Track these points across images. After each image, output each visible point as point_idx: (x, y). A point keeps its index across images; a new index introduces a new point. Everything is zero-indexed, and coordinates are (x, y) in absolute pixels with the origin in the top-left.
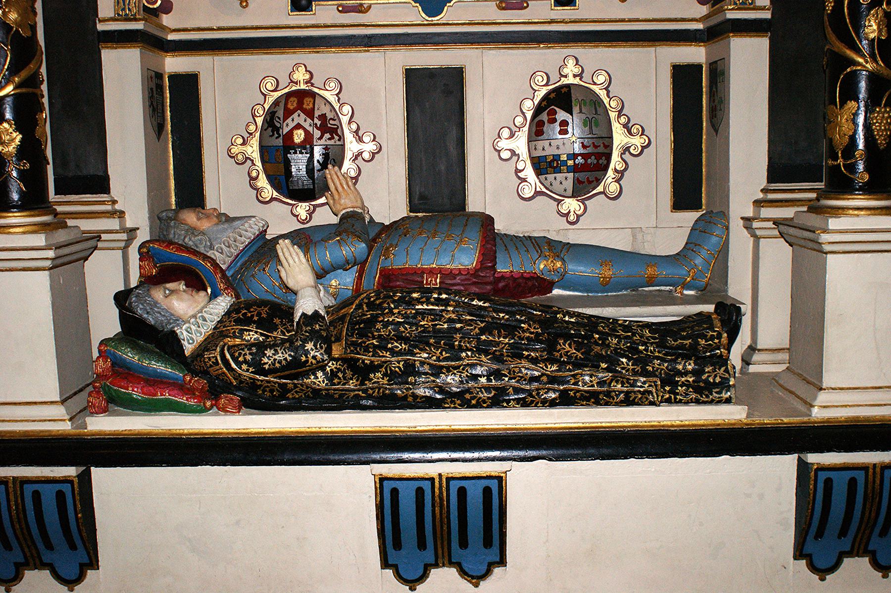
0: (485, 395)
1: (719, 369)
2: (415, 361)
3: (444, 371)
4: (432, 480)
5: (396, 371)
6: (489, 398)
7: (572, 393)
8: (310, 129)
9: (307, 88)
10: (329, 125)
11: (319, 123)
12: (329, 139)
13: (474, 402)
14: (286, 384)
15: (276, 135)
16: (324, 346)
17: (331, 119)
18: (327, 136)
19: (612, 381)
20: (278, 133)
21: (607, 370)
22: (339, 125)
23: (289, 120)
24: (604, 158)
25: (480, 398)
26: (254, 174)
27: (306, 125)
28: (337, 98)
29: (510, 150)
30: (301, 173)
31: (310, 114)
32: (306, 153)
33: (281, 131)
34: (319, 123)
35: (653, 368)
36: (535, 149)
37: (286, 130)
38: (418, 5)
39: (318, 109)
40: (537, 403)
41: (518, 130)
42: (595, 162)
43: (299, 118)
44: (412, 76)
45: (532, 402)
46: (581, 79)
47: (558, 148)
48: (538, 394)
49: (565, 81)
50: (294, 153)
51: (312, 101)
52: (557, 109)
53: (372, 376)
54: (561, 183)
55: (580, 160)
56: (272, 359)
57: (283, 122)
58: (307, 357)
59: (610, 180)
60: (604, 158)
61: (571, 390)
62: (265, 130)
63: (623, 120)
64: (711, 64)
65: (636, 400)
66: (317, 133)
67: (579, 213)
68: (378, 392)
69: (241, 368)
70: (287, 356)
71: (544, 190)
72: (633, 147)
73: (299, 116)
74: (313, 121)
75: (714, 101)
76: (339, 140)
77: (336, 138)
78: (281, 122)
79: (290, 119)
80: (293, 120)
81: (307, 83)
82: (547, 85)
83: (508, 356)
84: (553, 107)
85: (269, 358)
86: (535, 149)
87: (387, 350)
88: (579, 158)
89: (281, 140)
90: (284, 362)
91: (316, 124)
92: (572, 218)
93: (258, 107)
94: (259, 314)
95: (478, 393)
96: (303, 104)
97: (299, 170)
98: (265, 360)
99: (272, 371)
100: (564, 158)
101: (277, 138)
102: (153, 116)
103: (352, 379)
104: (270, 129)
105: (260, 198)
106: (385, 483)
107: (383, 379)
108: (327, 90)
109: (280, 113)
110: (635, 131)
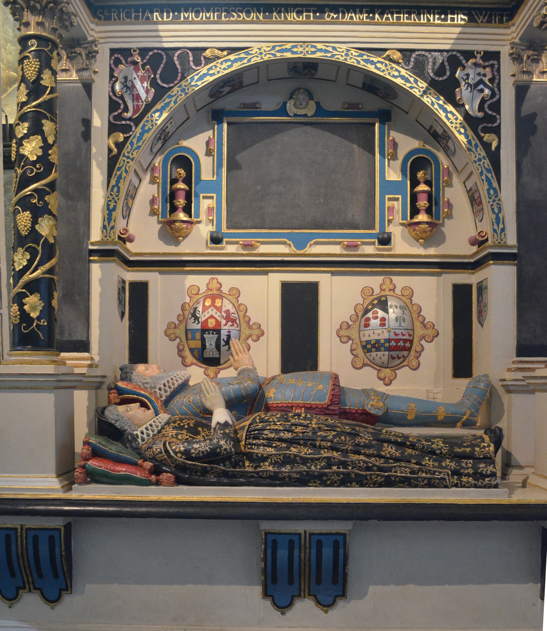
0: (335, 478)
1: (489, 466)
2: (291, 454)
3: (309, 461)
4: (300, 534)
5: (278, 461)
6: (339, 480)
7: (393, 478)
8: (219, 319)
11: (225, 315)
12: (231, 326)
13: (329, 482)
14: (206, 467)
15: (197, 322)
16: (232, 443)
17: (232, 313)
18: (230, 323)
19: (419, 471)
20: (198, 321)
21: (416, 464)
23: (206, 313)
24: (408, 343)
25: (333, 480)
26: (181, 348)
27: (217, 316)
29: (347, 336)
31: (219, 309)
33: (200, 320)
34: (225, 315)
35: (446, 464)
36: (364, 336)
37: (203, 319)
38: (291, 242)
40: (370, 484)
41: (352, 323)
42: (403, 344)
43: (212, 312)
44: (286, 287)
45: (367, 483)
46: (394, 292)
47: (379, 335)
48: (371, 478)
49: (383, 293)
50: (209, 334)
51: (221, 301)
52: (378, 310)
53: (262, 464)
54: (380, 358)
55: (393, 343)
56: (198, 451)
58: (220, 449)
59: (412, 358)
60: (408, 343)
61: (393, 476)
63: (421, 319)
64: (478, 283)
65: (435, 484)
66: (223, 322)
67: (391, 378)
68: (266, 475)
69: (177, 456)
70: (207, 448)
71: (369, 362)
72: (427, 337)
75: (480, 306)
76: (237, 327)
77: (236, 325)
79: (206, 312)
80: (208, 312)
81: (218, 290)
82: (372, 295)
83: (351, 453)
84: (376, 309)
85: (196, 449)
86: (364, 336)
87: (272, 447)
88: (393, 342)
89: (199, 325)
90: (205, 453)
91: (223, 316)
92: (387, 380)
94: (188, 424)
95: (331, 476)
96: (215, 303)
97: (211, 345)
98: (193, 451)
99: (197, 459)
100: (382, 341)
103: (248, 466)
104: (193, 318)
106: (269, 536)
107: (269, 466)
110: (429, 326)
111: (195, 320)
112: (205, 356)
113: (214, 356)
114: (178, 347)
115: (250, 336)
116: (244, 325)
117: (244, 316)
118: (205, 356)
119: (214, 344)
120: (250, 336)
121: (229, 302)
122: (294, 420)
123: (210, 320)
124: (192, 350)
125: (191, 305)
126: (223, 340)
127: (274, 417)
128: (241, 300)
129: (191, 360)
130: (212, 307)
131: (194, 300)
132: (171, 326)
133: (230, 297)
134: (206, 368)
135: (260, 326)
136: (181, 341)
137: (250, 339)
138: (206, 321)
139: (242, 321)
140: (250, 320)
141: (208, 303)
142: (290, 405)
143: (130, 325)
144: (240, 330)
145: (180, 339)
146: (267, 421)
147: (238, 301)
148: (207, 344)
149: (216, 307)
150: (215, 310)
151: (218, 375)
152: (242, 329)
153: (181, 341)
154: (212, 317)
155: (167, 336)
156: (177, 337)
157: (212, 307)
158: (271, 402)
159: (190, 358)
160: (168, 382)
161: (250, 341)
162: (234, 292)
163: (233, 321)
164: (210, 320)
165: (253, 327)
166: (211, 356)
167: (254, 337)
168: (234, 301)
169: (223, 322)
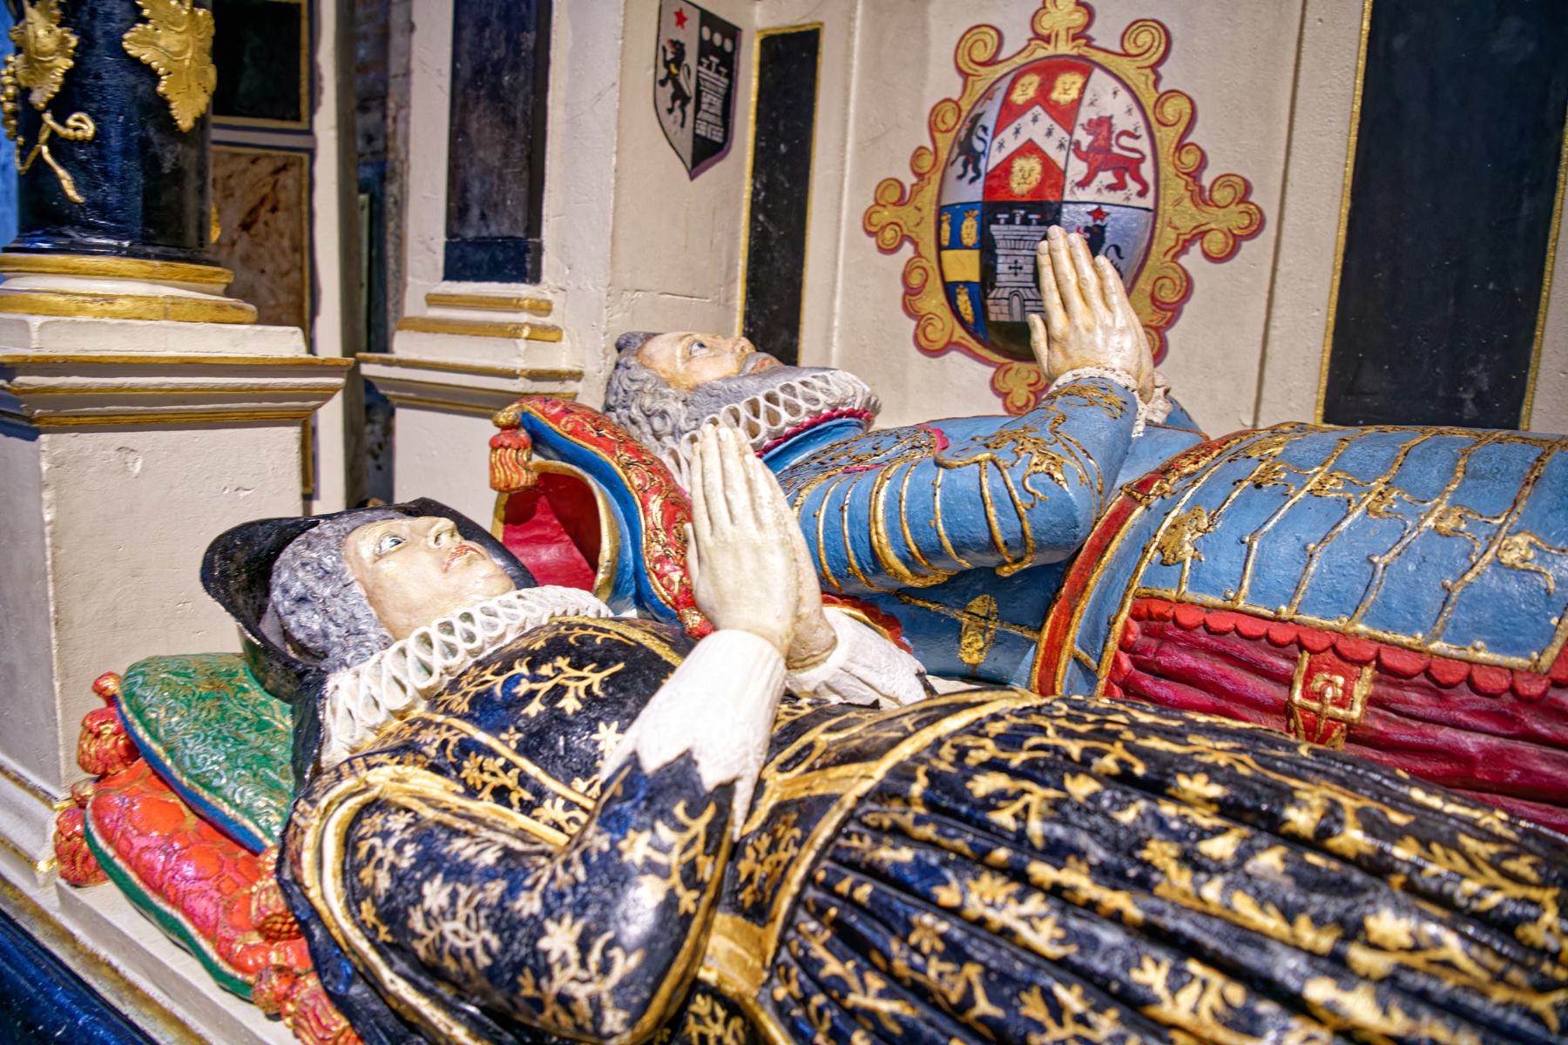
8: (1058, 157)
9: (1074, 52)
10: (1116, 150)
11: (1085, 140)
12: (1111, 187)
15: (971, 174)
20: (976, 170)
22: (1147, 150)
23: (1007, 134)
26: (916, 280)
28: (1152, 77)
30: (1019, 278)
31: (1065, 116)
33: (983, 161)
34: (1085, 140)
37: (995, 158)
39: (1092, 104)
43: (1036, 127)
50: (1010, 221)
57: (995, 135)
66: (1077, 169)
73: (1035, 120)
74: (1071, 133)
76: (1142, 194)
77: (1134, 187)
79: (1011, 130)
80: (1017, 131)
89: (980, 183)
91: (1078, 144)
93: (950, 106)
96: (1051, 89)
105: (924, 343)
108: (1127, 55)
111: (965, 166)
112: (993, 318)
114: (905, 278)
115: (1200, 235)
116: (1175, 187)
117: (1180, 147)
118: (993, 318)
120: (1200, 235)
121: (1115, 84)
122: (1182, 879)
123: (1019, 164)
125: (966, 106)
127: (1037, 796)
128: (1172, 75)
129: (948, 331)
130: (1038, 109)
131: (980, 87)
132: (893, 195)
133: (1126, 67)
135: (1248, 188)
137: (1195, 250)
138: (1005, 167)
139: (1168, 170)
140: (1203, 163)
142: (1280, 634)
143: (755, 193)
144: (1154, 212)
145: (915, 244)
146: (976, 815)
148: (1002, 267)
149: (1055, 110)
150: (1046, 121)
152: (1166, 207)
153: (918, 254)
154: (1030, 149)
155: (870, 234)
156: (905, 238)
157: (1038, 109)
158: (1173, 594)
159: (944, 326)
161: (1193, 260)
162: (1145, 38)
163: (1126, 168)
164: (1019, 164)
165: (1217, 196)
167: (1216, 242)
168: (1141, 82)
169: (1077, 169)
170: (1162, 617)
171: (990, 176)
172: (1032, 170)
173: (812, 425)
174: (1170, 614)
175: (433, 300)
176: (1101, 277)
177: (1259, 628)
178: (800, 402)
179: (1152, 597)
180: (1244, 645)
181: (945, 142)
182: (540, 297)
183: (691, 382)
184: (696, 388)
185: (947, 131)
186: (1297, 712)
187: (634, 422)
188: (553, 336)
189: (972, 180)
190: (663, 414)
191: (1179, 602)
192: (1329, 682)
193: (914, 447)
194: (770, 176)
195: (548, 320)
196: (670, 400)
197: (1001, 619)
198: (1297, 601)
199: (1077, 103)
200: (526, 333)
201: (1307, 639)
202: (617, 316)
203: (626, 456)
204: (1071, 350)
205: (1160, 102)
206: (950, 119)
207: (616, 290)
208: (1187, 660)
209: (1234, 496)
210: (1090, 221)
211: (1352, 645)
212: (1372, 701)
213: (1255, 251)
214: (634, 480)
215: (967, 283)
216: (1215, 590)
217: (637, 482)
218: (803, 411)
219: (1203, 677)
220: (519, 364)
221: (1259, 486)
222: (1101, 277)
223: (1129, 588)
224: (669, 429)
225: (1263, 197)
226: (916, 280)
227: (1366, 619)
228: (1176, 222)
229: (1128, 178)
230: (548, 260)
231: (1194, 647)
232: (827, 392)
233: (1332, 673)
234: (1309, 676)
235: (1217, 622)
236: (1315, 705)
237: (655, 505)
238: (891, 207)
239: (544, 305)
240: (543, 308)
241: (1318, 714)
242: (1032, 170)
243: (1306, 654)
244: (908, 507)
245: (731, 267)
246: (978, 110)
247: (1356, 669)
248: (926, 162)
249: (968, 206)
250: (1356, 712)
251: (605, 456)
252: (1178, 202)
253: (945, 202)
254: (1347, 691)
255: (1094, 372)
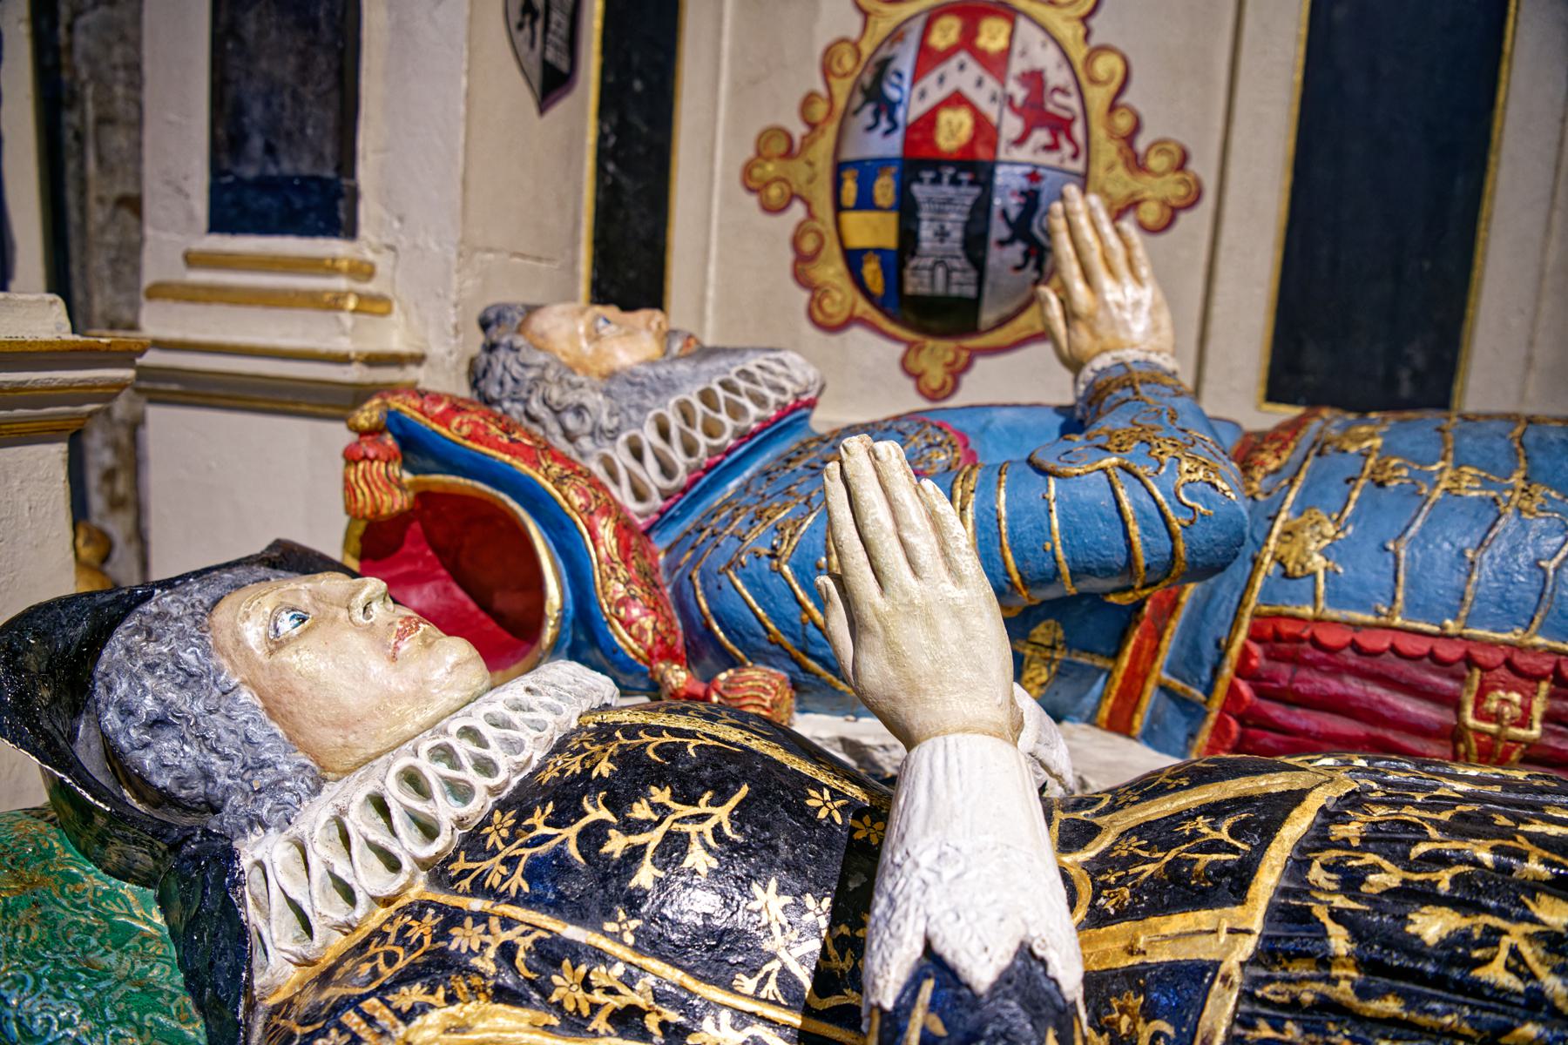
8: (991, 111)
10: (1050, 107)
11: (1020, 94)
15: (884, 125)
17: (1056, 89)
18: (1041, 136)
23: (930, 81)
26: (809, 245)
27: (981, 99)
28: (1081, 31)
31: (995, 64)
32: (972, 183)
33: (900, 114)
34: (1020, 94)
37: (917, 109)
43: (962, 75)
50: (937, 181)
62: (856, 112)
66: (1011, 126)
73: (962, 67)
74: (1003, 84)
76: (1075, 156)
77: (1067, 148)
78: (906, 86)
80: (941, 80)
89: (897, 139)
93: (846, 48)
101: (887, 133)
102: (520, 26)
104: (869, 108)
105: (819, 316)
109: (905, 61)
111: (876, 114)
113: (955, 291)
114: (796, 243)
117: (1113, 107)
119: (957, 234)
123: (945, 116)
124: (853, 259)
125: (867, 48)
126: (1004, 214)
129: (848, 306)
131: (883, 27)
134: (910, 345)
136: (811, 215)
138: (929, 121)
139: (1099, 133)
140: (1137, 127)
141: (946, 33)
142: (1447, 651)
143: (602, 138)
145: (808, 204)
147: (1087, 35)
148: (926, 231)
149: (981, 57)
150: (974, 70)
151: (967, 380)
153: (811, 215)
154: (957, 100)
155: (751, 190)
156: (793, 196)
157: (963, 56)
158: (1308, 611)
159: (842, 296)
160: (686, 412)
163: (1060, 126)
164: (945, 116)
166: (940, 289)
168: (1069, 31)
170: (1298, 639)
171: (910, 129)
172: (961, 125)
173: (779, 419)
174: (1307, 633)
175: (193, 260)
176: (1127, 246)
177: (1422, 646)
178: (766, 392)
179: (1279, 616)
180: (1404, 665)
181: (842, 88)
182: (358, 256)
183: (604, 367)
184: (611, 375)
185: (845, 75)
186: (1471, 736)
187: (533, 419)
188: (379, 308)
189: (887, 133)
190: (579, 410)
191: (1318, 620)
192: (1505, 701)
193: (930, 446)
194: (622, 118)
195: (371, 287)
196: (586, 390)
197: (1069, 645)
198: (1463, 614)
199: (1006, 53)
200: (351, 303)
201: (1480, 655)
202: (469, 283)
203: (556, 469)
204: (1102, 329)
205: (1090, 59)
206: (848, 62)
207: (467, 249)
208: (1334, 686)
209: (1355, 495)
210: (1024, 184)
211: (1530, 660)
212: (1548, 718)
213: (1195, 223)
214: (573, 499)
215: (878, 251)
216: (1362, 606)
217: (578, 501)
218: (772, 403)
219: (1354, 704)
220: (344, 345)
221: (1381, 484)
222: (1127, 246)
223: (1241, 603)
224: (588, 428)
225: (1204, 167)
226: (809, 245)
227: (1542, 630)
228: (1110, 188)
229: (1062, 139)
230: (368, 210)
231: (1339, 670)
232: (789, 377)
233: (1508, 690)
234: (1481, 695)
235: (1369, 641)
236: (1492, 727)
237: (606, 530)
238: (777, 161)
239: (366, 268)
240: (363, 271)
241: (1495, 737)
242: (961, 125)
243: (1477, 672)
244: (1011, 529)
245: (577, 224)
246: (883, 53)
247: (1533, 685)
248: (820, 110)
249: (882, 163)
250: (1536, 732)
251: (523, 467)
252: (1111, 167)
253: (849, 154)
254: (1527, 710)
255: (1141, 356)
